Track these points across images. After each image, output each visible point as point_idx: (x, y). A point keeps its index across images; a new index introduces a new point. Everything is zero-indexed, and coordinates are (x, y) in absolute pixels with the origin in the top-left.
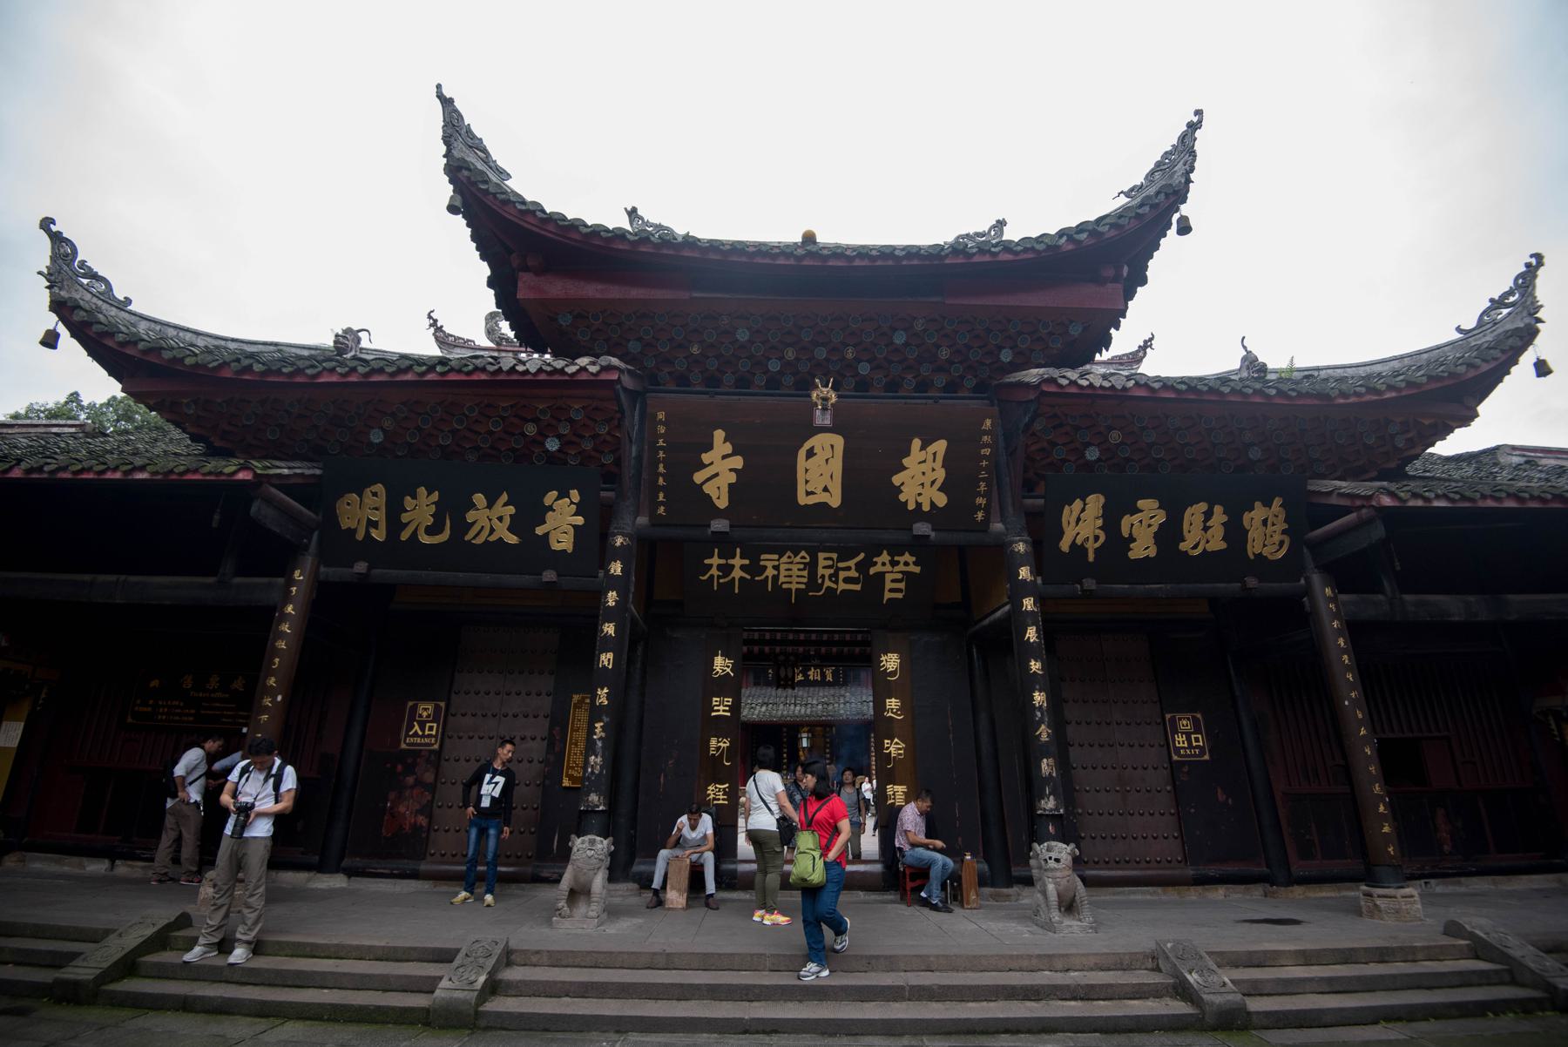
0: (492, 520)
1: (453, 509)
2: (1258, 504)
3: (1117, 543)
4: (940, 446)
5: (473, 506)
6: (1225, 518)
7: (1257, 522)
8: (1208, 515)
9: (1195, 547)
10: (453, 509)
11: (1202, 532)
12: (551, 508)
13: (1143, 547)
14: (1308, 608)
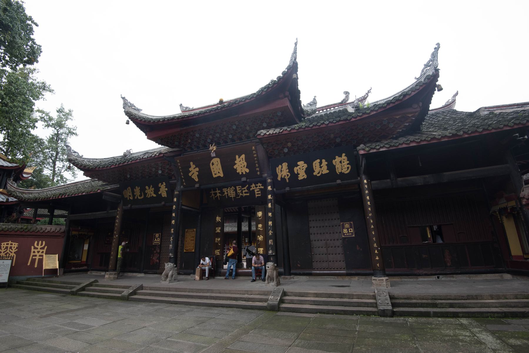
0: (150, 192)
1: (143, 190)
2: (337, 157)
3: (294, 176)
4: (243, 156)
6: (326, 163)
7: (338, 162)
8: (321, 163)
9: (319, 173)
11: (320, 168)
13: (302, 176)
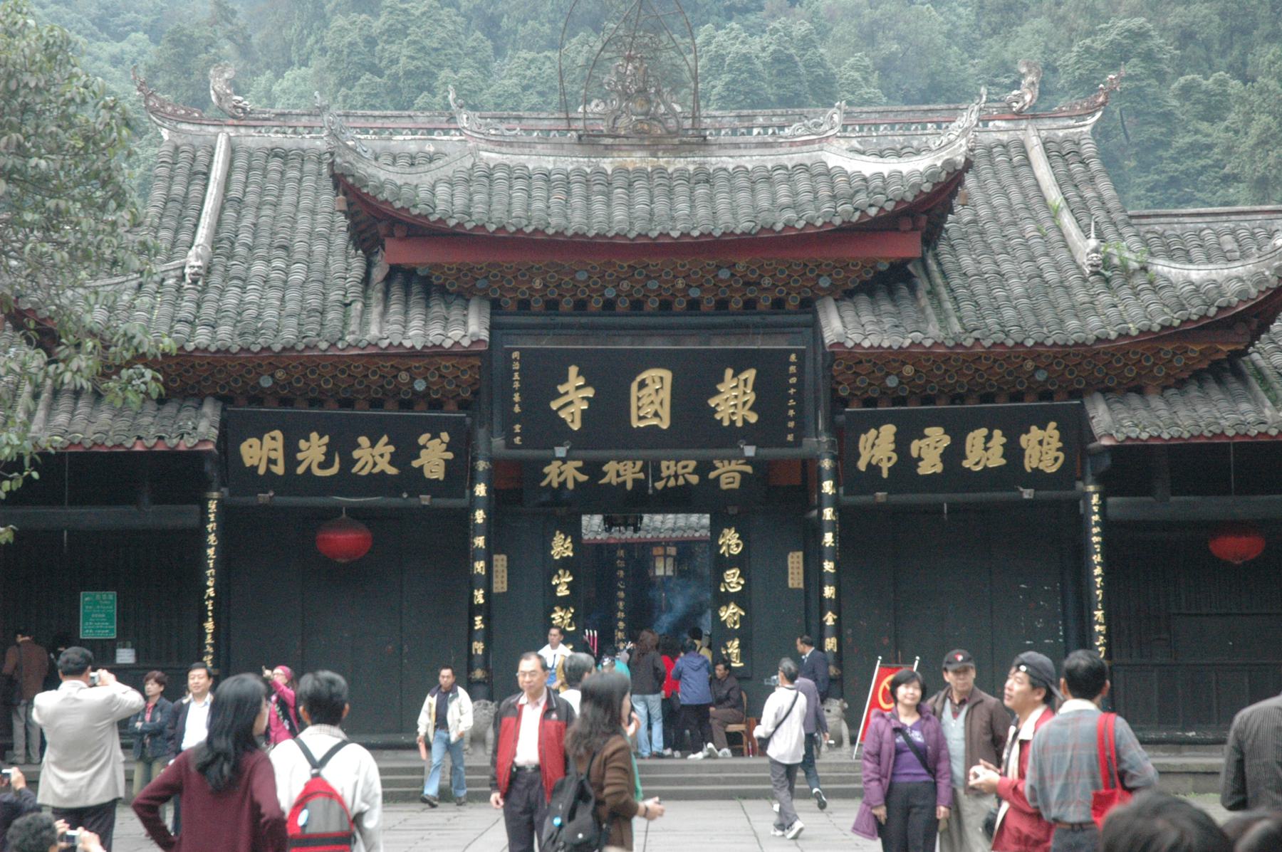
0: (374, 456)
1: (341, 447)
3: (906, 462)
5: (358, 446)
6: (1004, 440)
7: (1034, 443)
8: (988, 438)
9: (977, 464)
10: (341, 447)
11: (984, 451)
12: (425, 447)
13: (930, 464)
14: (1082, 511)
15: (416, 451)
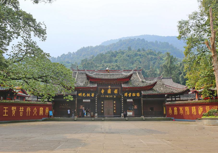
1: (86, 94)
3: (128, 96)
10: (86, 94)
13: (130, 96)
15: (91, 94)
